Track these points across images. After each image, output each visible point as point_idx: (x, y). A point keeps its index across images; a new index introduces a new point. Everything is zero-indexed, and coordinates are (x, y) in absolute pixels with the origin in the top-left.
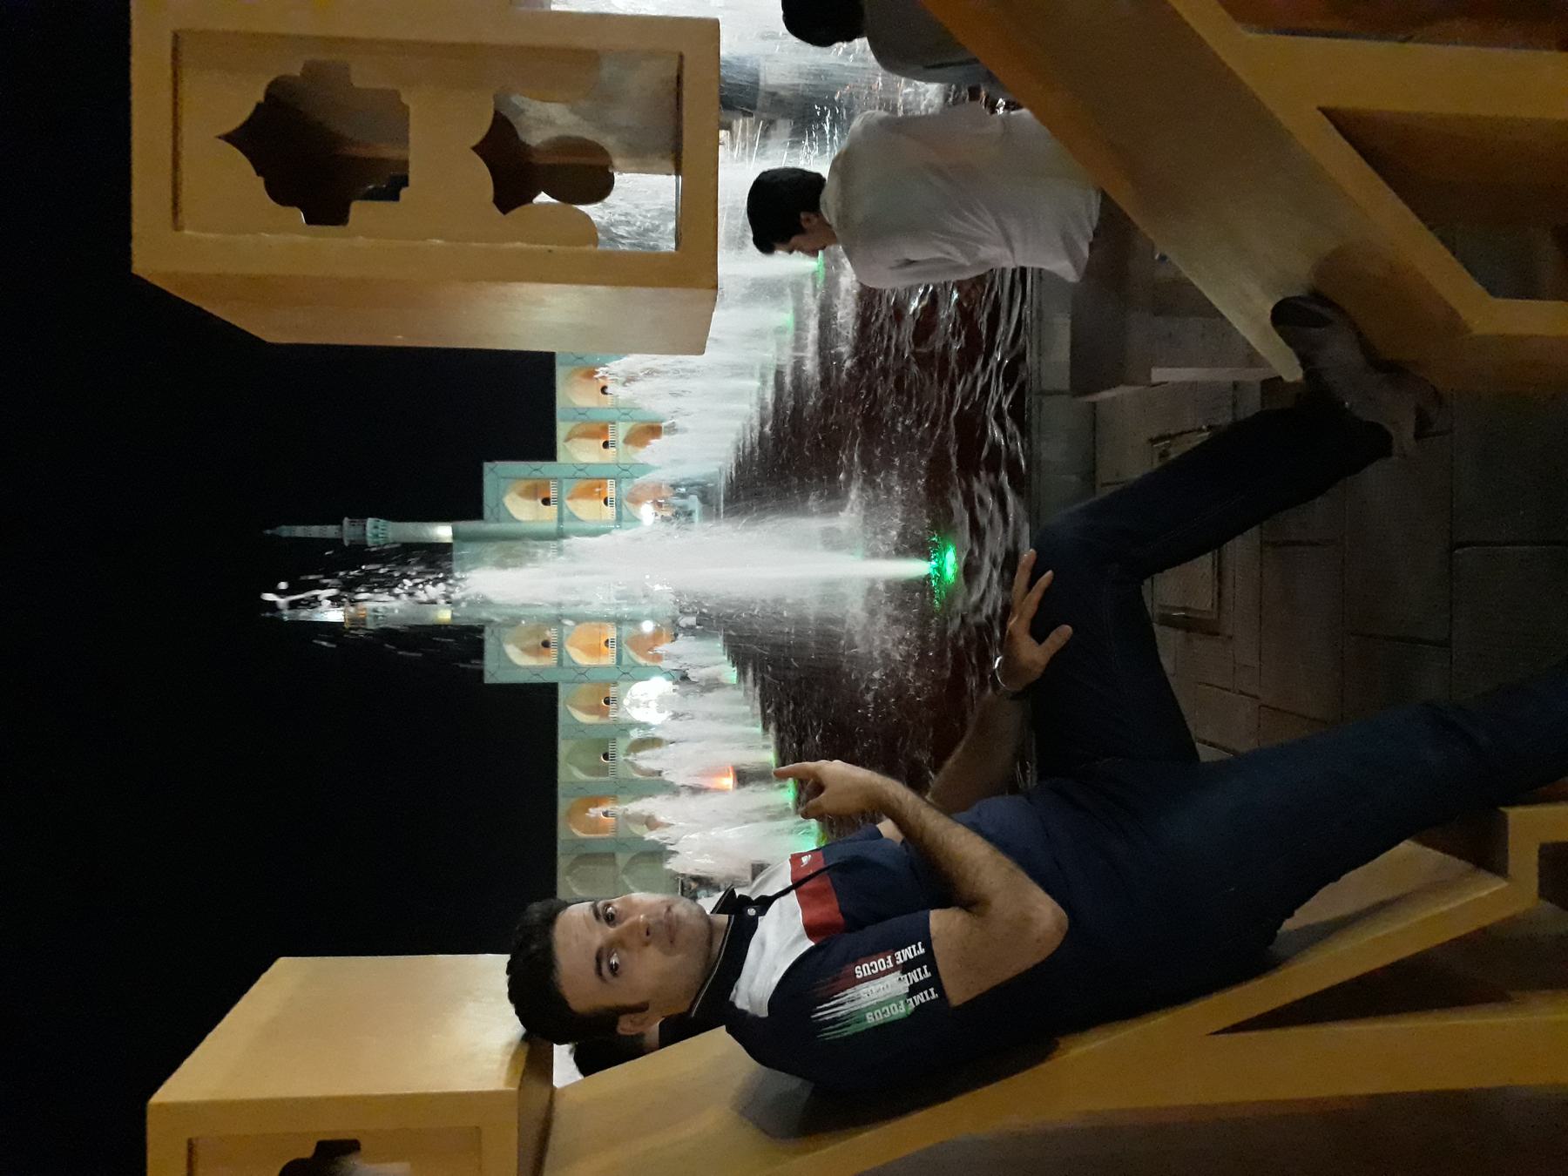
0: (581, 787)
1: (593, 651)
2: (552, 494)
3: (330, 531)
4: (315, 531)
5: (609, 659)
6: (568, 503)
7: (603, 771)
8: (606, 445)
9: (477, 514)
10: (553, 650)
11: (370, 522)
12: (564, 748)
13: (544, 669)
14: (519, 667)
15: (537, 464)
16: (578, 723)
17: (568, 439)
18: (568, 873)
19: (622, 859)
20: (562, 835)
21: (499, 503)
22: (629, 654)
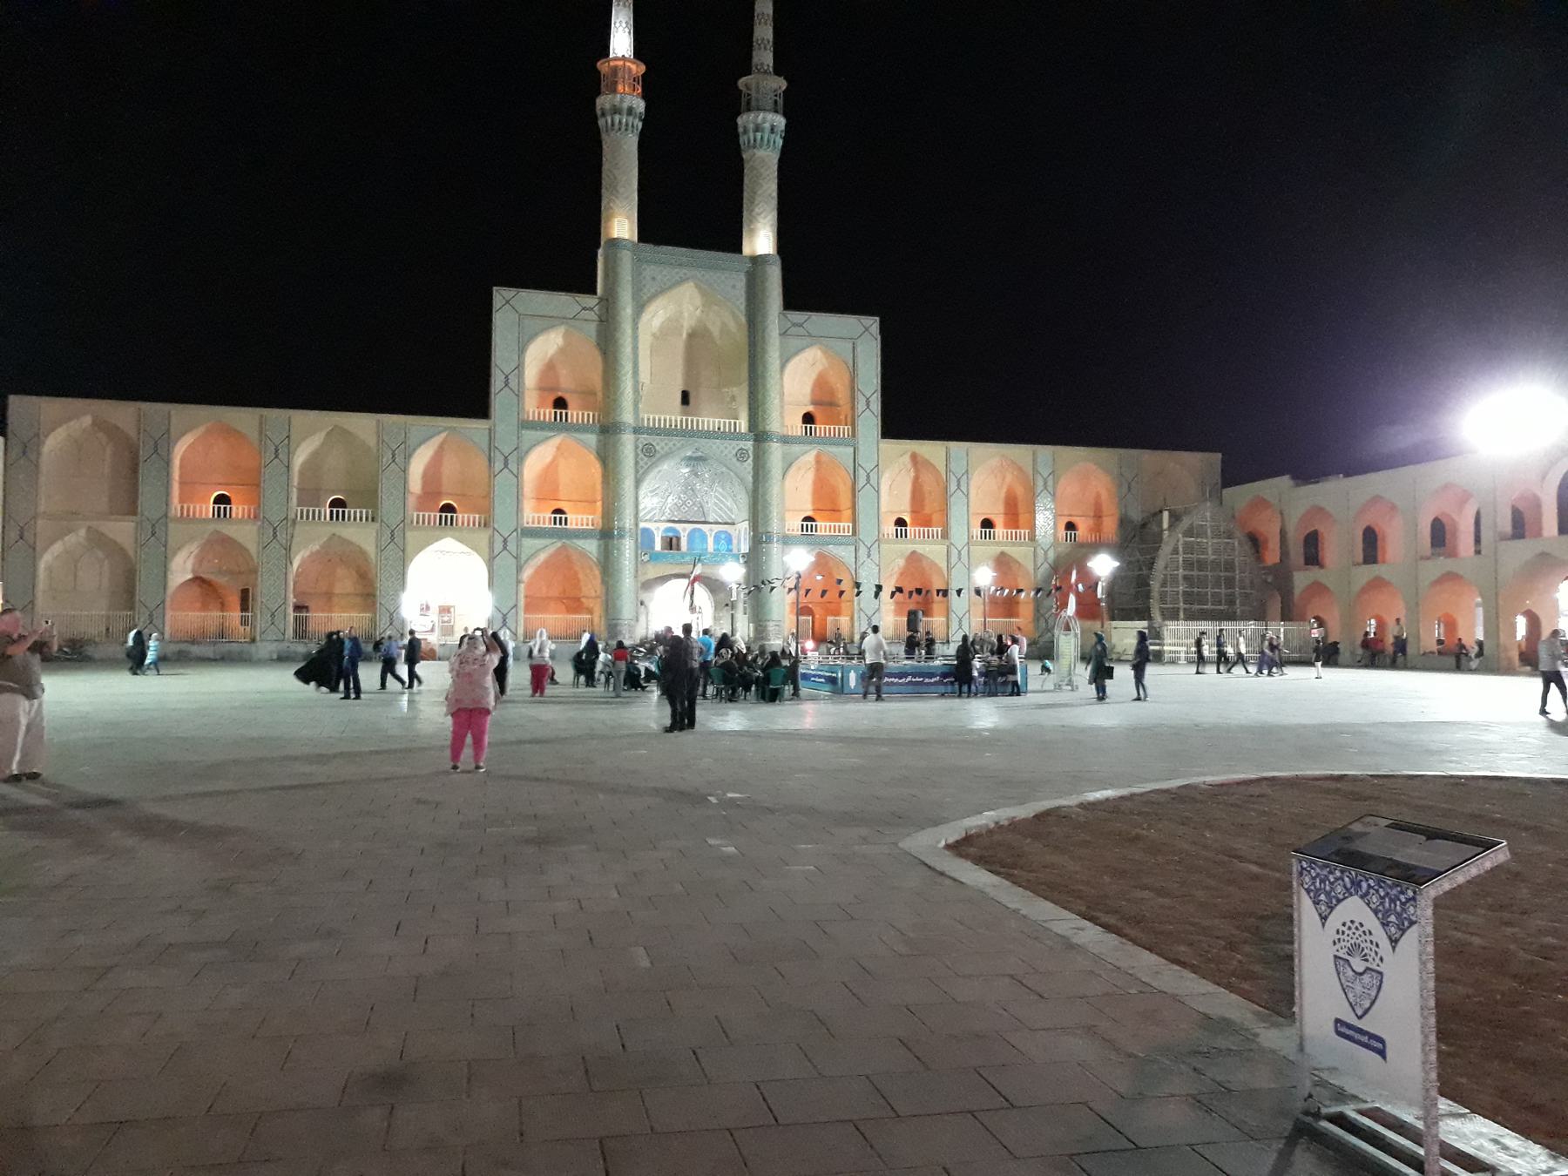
0: (283, 451)
1: (548, 487)
2: (820, 428)
3: (764, 57)
4: (764, 32)
5: (534, 515)
6: (810, 457)
7: (310, 496)
9: (795, 299)
10: (549, 412)
11: (780, 121)
12: (363, 425)
13: (519, 395)
14: (522, 351)
15: (876, 406)
16: (408, 457)
17: (914, 457)
18: (98, 424)
19: (122, 530)
20: (179, 413)
21: (813, 338)
22: (540, 553)
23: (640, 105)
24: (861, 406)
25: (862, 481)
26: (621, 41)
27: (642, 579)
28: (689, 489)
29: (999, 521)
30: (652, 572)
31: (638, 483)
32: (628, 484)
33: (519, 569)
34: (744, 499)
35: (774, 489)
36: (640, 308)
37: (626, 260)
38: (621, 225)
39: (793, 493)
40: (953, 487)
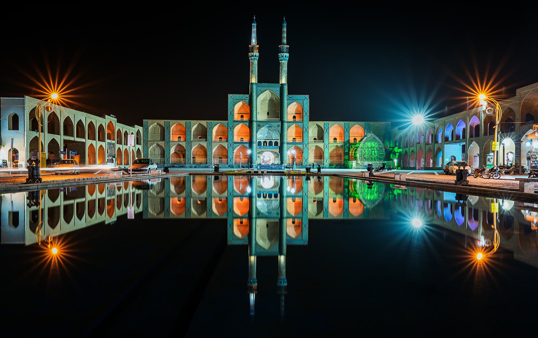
6: (294, 125)
8: (315, 139)
9: (289, 93)
11: (287, 55)
14: (234, 106)
15: (308, 114)
18: (158, 124)
19: (162, 143)
21: (294, 100)
23: (258, 54)
24: (304, 114)
25: (304, 130)
26: (254, 41)
27: (258, 152)
28: (268, 133)
29: (338, 138)
30: (260, 150)
31: (257, 132)
32: (254, 133)
33: (233, 150)
34: (279, 135)
35: (285, 133)
36: (257, 96)
37: (254, 87)
38: (254, 80)
39: (290, 133)
40: (325, 131)
